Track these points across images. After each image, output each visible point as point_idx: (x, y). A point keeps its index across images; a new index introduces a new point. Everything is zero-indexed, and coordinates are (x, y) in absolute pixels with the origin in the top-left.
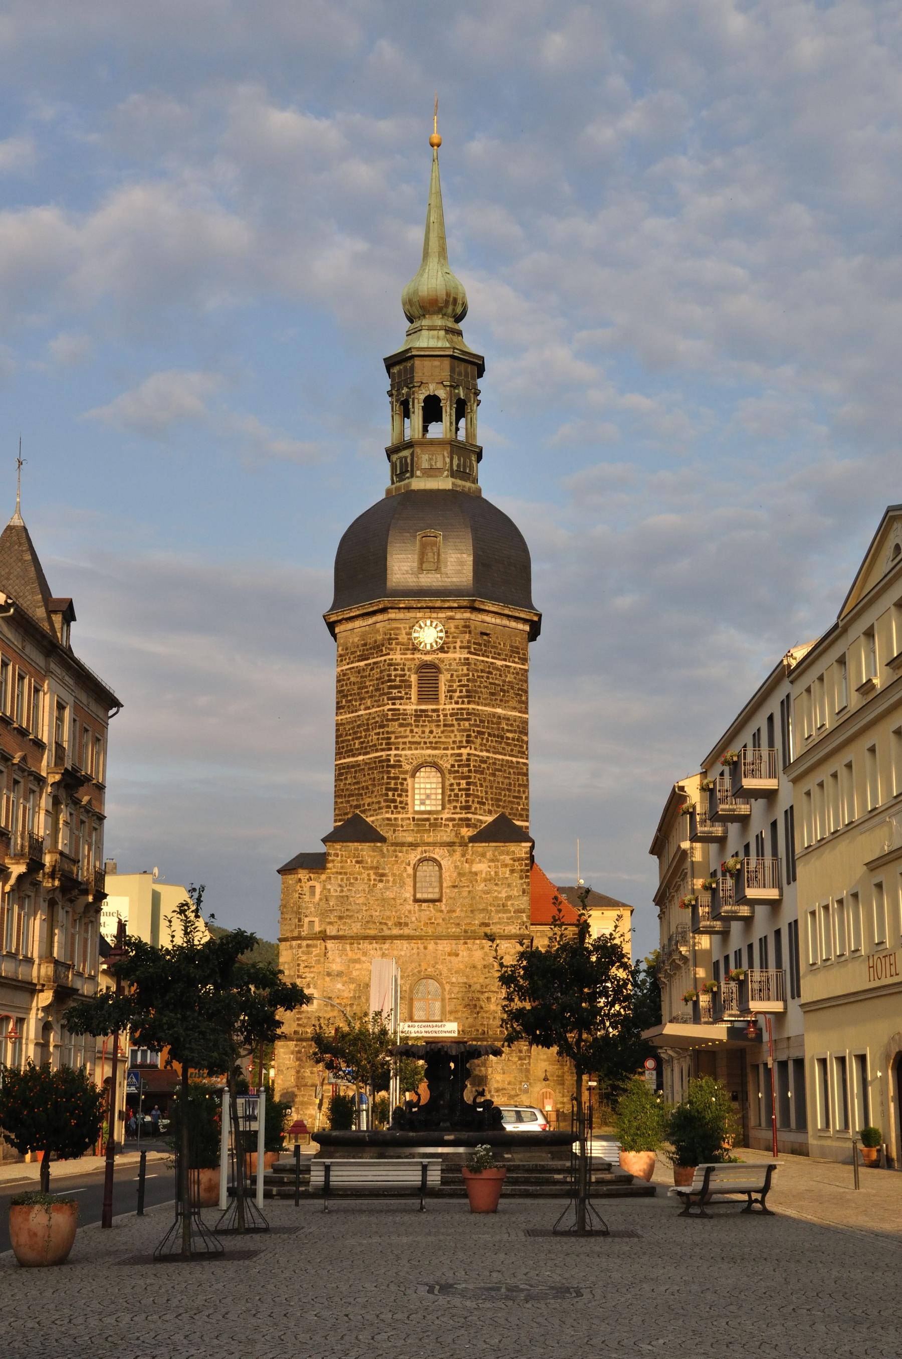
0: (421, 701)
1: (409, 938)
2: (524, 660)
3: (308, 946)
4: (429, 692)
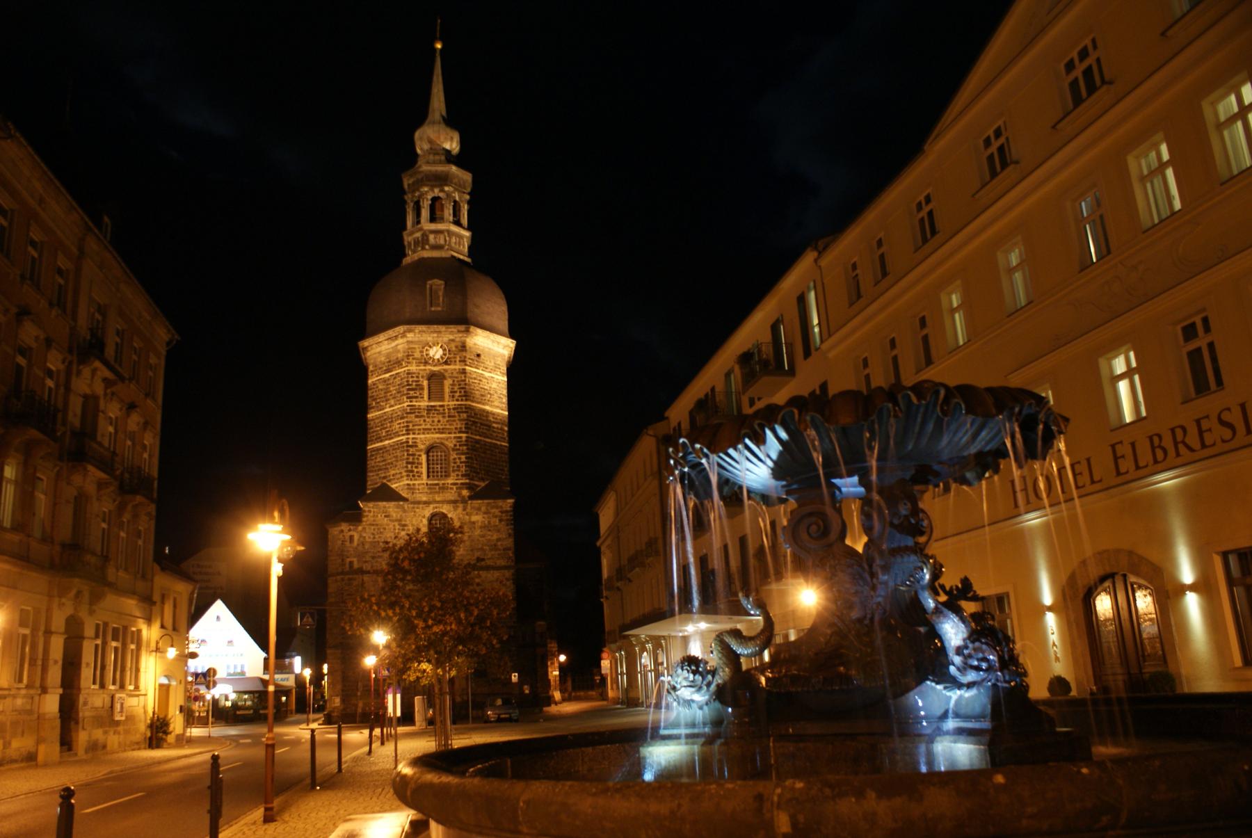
3: (350, 579)
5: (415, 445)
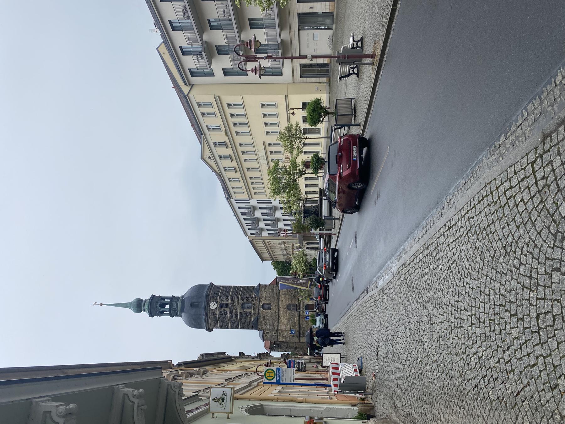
1: (279, 311)
4: (226, 306)
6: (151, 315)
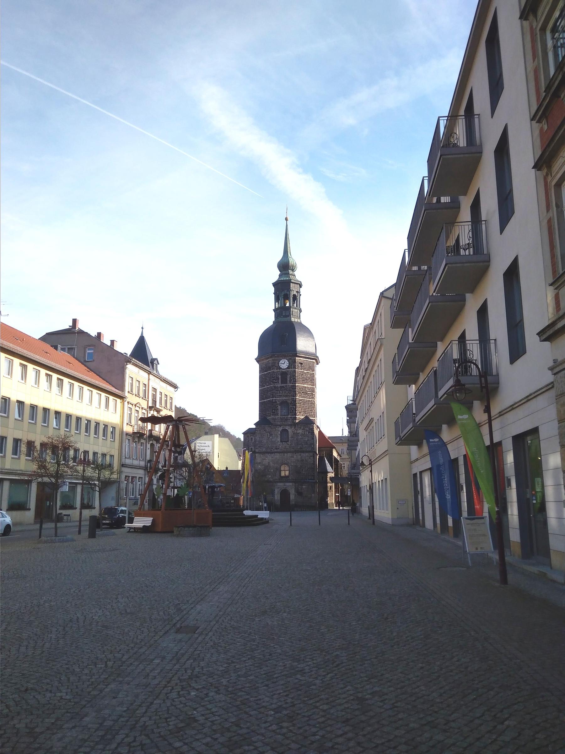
0: (282, 383)
1: (279, 452)
2: (313, 370)
5: (276, 402)
6: (275, 285)
